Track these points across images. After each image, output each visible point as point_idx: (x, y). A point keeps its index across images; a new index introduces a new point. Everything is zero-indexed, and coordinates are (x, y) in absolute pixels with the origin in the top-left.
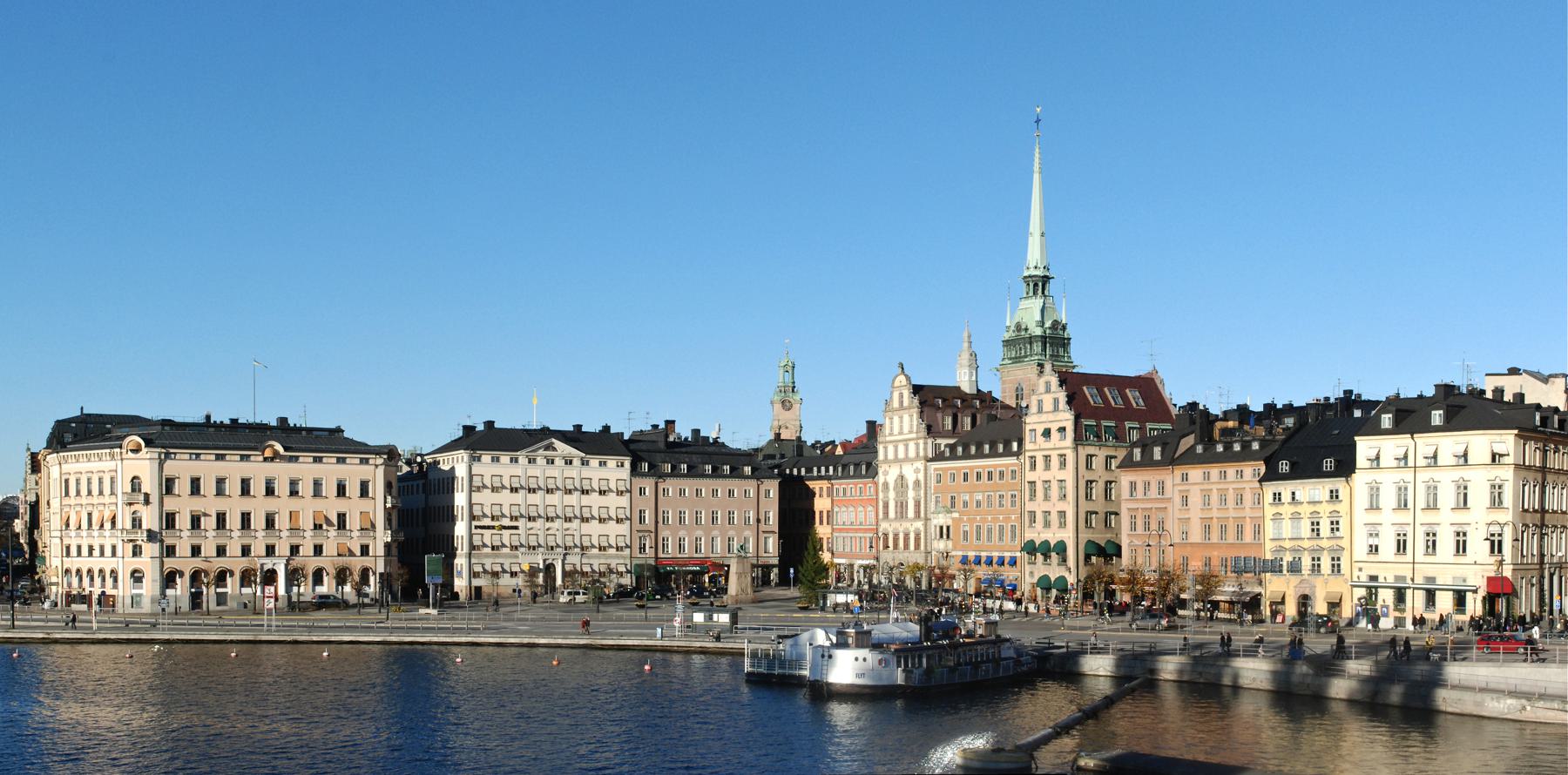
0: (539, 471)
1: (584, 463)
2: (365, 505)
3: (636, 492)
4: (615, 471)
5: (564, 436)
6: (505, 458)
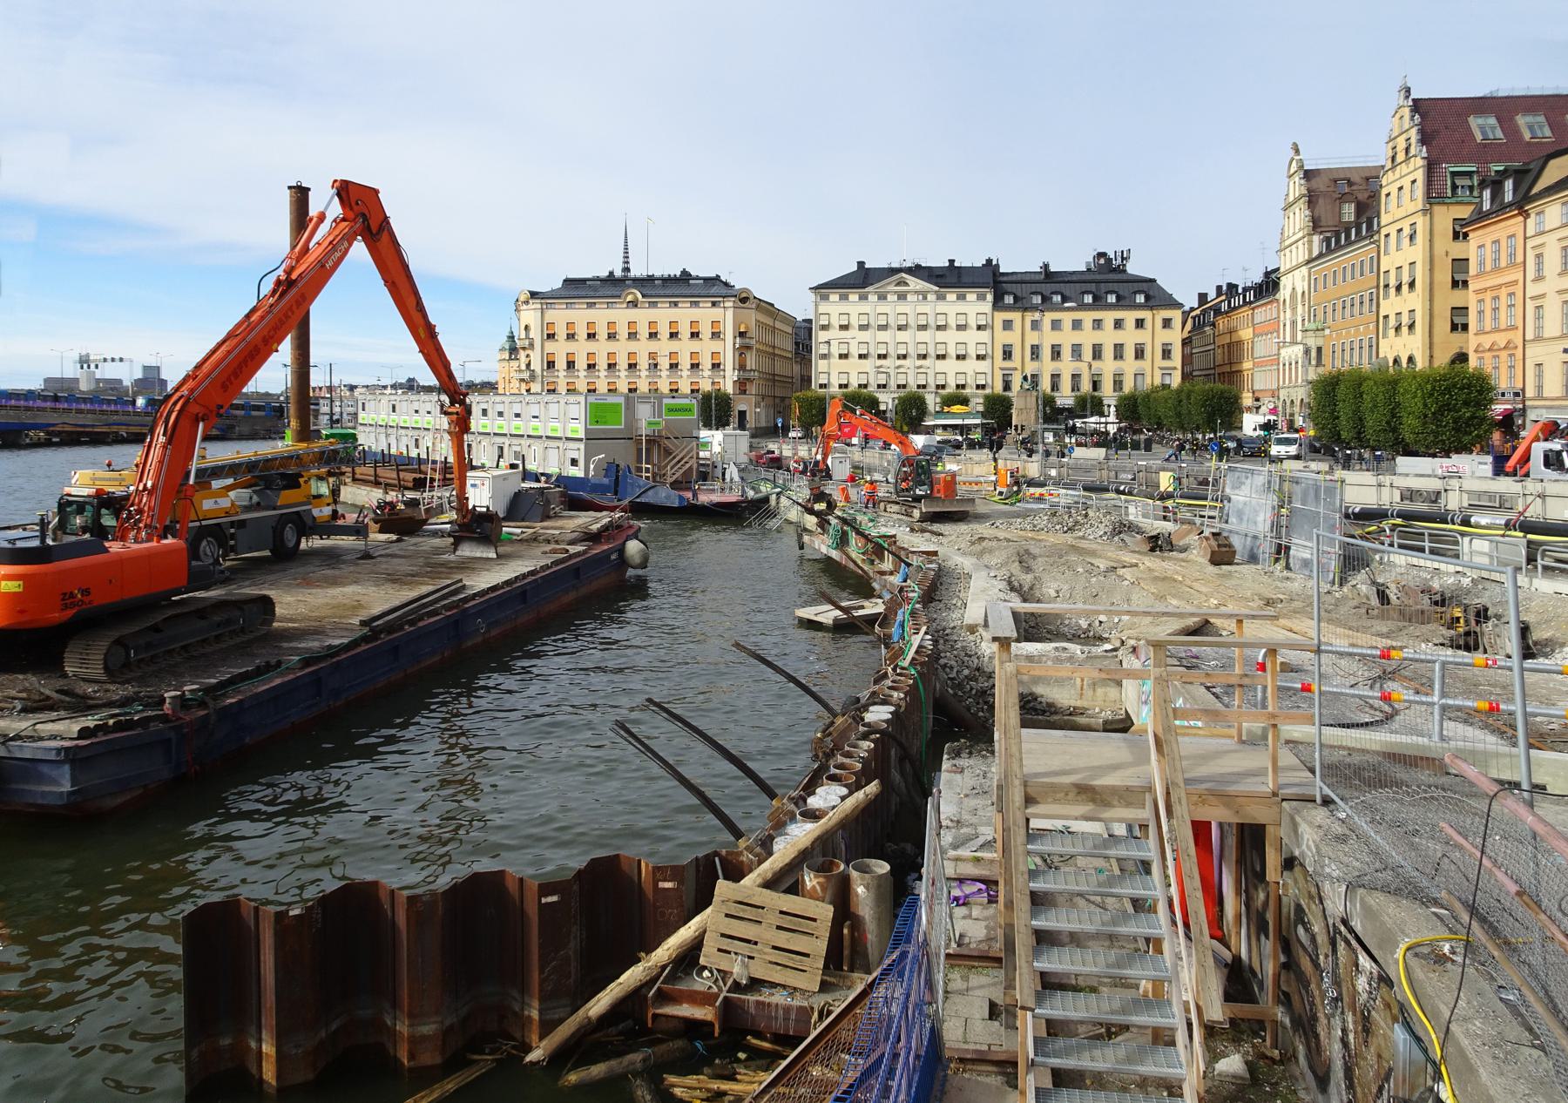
0: (892, 309)
1: (941, 297)
2: (716, 346)
3: (998, 325)
4: (976, 306)
5: (909, 271)
6: (854, 297)
